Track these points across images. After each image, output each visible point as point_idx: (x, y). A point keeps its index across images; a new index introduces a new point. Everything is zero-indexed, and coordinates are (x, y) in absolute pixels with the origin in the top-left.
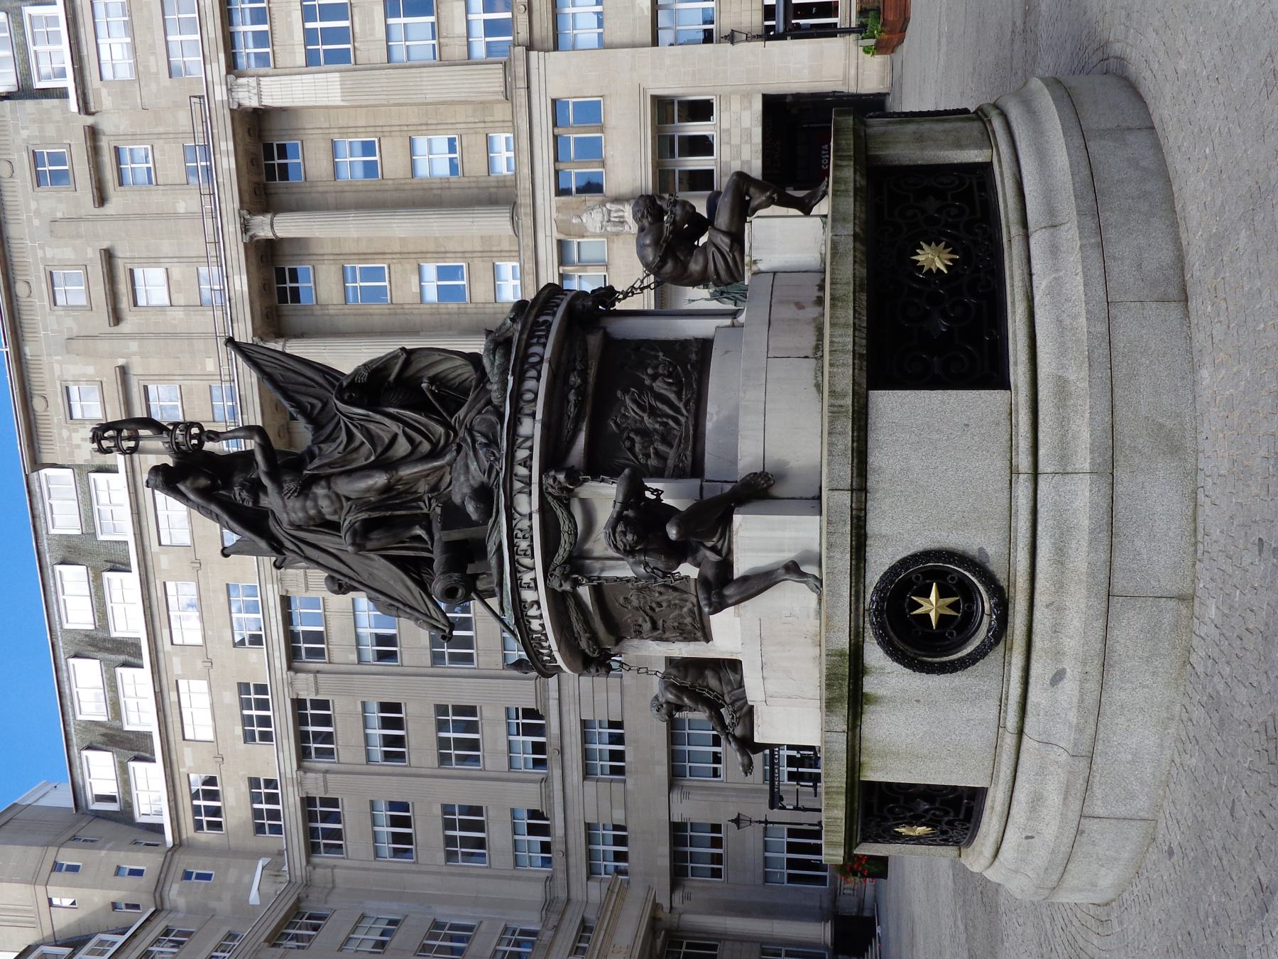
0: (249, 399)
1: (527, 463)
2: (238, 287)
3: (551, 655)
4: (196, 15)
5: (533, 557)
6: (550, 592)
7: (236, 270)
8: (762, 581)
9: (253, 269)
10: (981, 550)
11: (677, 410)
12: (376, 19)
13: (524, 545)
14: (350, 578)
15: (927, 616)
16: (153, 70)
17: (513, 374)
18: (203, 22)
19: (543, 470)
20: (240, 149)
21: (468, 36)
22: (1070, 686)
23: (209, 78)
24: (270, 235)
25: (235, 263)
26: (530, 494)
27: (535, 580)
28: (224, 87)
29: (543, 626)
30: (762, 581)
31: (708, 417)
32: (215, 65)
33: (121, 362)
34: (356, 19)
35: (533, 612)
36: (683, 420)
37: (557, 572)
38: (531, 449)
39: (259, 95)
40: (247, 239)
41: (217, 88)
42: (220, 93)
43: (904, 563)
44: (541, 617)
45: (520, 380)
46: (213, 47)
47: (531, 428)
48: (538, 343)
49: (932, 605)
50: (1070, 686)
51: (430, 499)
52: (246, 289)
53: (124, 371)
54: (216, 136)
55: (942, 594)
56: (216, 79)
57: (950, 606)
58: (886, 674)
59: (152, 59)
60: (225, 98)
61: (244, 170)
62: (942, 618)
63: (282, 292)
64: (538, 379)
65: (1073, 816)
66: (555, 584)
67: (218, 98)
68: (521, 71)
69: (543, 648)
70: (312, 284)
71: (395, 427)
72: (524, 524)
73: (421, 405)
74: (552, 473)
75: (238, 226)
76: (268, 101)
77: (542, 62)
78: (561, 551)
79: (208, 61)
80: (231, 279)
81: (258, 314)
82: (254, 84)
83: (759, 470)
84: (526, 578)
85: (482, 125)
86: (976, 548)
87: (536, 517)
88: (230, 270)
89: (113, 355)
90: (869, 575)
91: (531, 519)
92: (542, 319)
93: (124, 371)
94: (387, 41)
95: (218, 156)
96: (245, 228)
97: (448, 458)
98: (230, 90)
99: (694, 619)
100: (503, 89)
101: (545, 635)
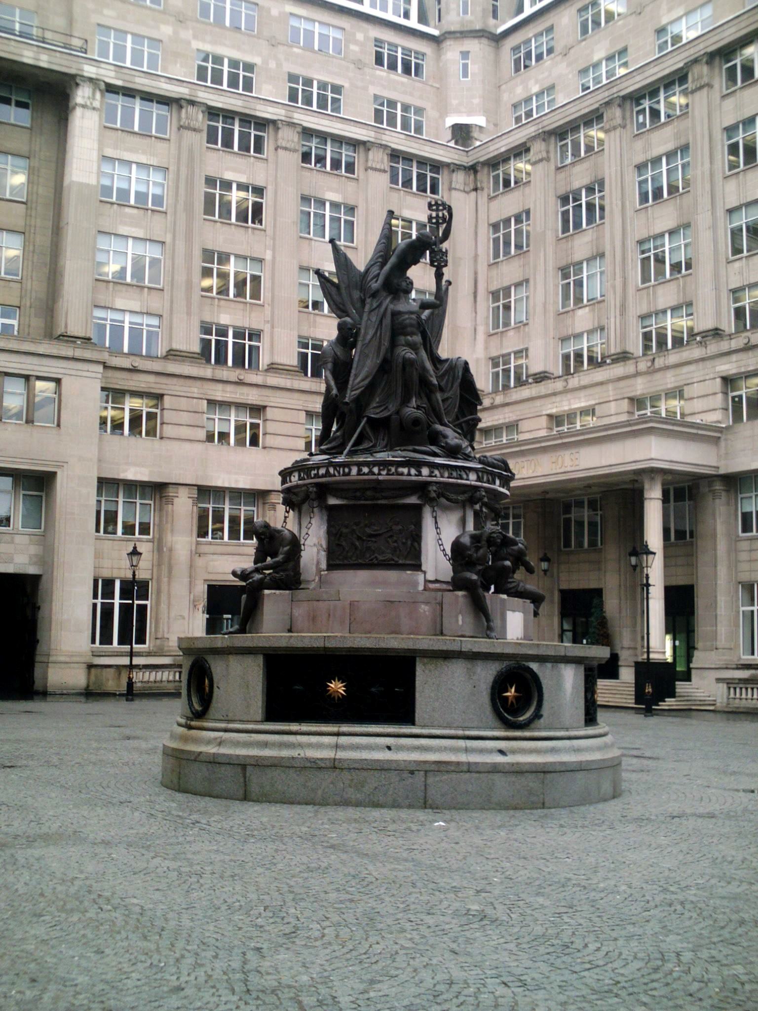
6: (430, 483)
12: (133, 229)
16: (106, 12)
19: (487, 490)
21: (111, 308)
22: (500, 759)
23: (103, 65)
27: (435, 476)
28: (93, 76)
32: (113, 74)
34: (135, 211)
35: (413, 471)
39: (84, 106)
42: (89, 70)
46: (127, 78)
49: (511, 693)
54: (53, 53)
56: (102, 72)
57: (512, 702)
58: (487, 673)
60: (86, 74)
65: (427, 767)
68: (87, 354)
69: (380, 470)
77: (94, 375)
79: (117, 69)
85: (28, 304)
94: (115, 234)
95: (35, 49)
98: (91, 80)
100: (69, 334)
101: (392, 474)
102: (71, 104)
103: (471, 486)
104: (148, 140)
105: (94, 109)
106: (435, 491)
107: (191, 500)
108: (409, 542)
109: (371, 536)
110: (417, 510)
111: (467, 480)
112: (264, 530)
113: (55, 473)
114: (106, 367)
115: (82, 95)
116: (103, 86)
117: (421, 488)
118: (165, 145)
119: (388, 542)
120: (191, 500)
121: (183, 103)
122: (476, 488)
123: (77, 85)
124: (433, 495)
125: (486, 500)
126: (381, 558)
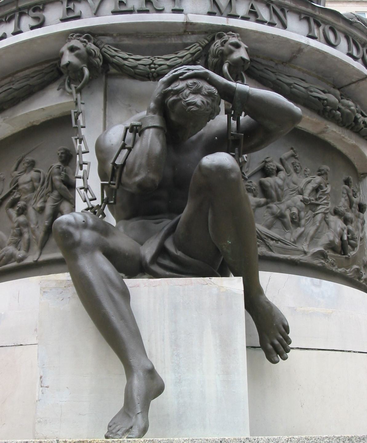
5: (115, 13)
26: (210, 13)
27: (78, 17)
30: (115, 333)
37: (91, 46)
38: (272, 24)
44: (17, 32)
83: (296, 337)
87: (179, 18)
91: (175, 11)
103: (189, 28)
119: (10, 217)
125: (242, 53)
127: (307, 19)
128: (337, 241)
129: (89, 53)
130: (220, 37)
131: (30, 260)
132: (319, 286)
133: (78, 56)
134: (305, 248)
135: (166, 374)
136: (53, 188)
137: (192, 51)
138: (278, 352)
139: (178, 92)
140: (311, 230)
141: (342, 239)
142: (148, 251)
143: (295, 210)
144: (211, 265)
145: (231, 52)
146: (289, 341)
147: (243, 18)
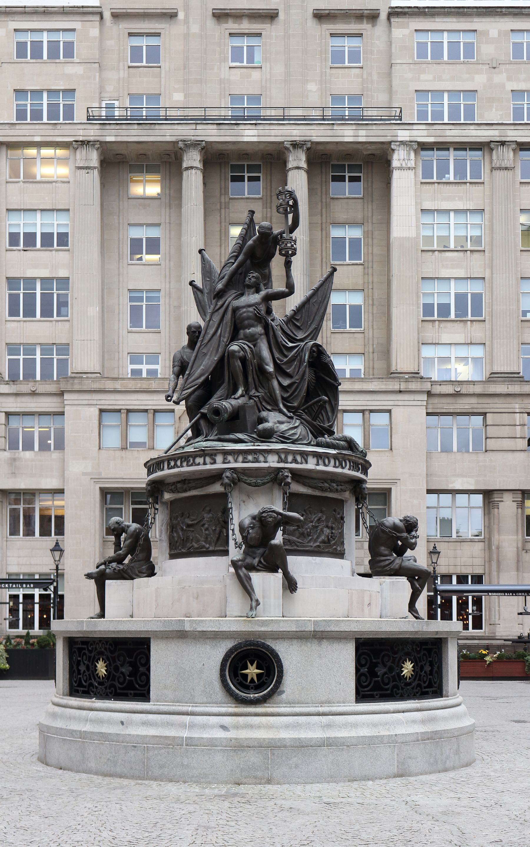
0: (151, 132)
1: (295, 461)
2: (247, 132)
3: (176, 466)
4: (462, 121)
5: (243, 462)
6: (224, 470)
7: (262, 133)
8: (247, 588)
9: (261, 147)
10: (283, 692)
11: (315, 541)
13: (250, 458)
14: (202, 341)
15: (247, 668)
17: (338, 453)
18: (458, 127)
19: (291, 470)
20: (359, 146)
23: (415, 127)
24: (290, 165)
25: (267, 132)
26: (278, 462)
27: (229, 462)
28: (408, 139)
29: (199, 464)
30: (247, 588)
31: (314, 558)
32: (425, 133)
33: (181, 15)
35: (208, 460)
36: (311, 544)
38: (302, 463)
39: (401, 168)
40: (287, 145)
41: (407, 133)
42: (403, 135)
43: (277, 656)
44: (205, 464)
45: (335, 457)
46: (438, 133)
47: (311, 465)
48: (350, 467)
49: (252, 671)
50: (221, 734)
51: (258, 396)
52: (246, 139)
53: (172, 16)
54: (370, 127)
55: (258, 675)
57: (252, 679)
59: (430, 77)
60: (400, 139)
61: (341, 148)
62: (246, 676)
63: (241, 168)
64: (335, 466)
66: (228, 474)
67: (400, 133)
70: (246, 196)
71: (296, 378)
72: (261, 458)
73: (309, 395)
74: (290, 475)
75: (297, 139)
76: (396, 175)
78: (245, 478)
80: (253, 127)
81: (224, 147)
82: (409, 165)
84: (230, 458)
86: (285, 689)
88: (261, 127)
89: (187, 8)
90: (270, 640)
91: (265, 462)
92: (360, 466)
93: (172, 16)
95: (354, 127)
96: (296, 145)
97: (285, 410)
99: (197, 548)
101: (192, 465)
102: (391, 169)
104: (463, 187)
105: (409, 168)
106: (227, 477)
107: (515, 504)
108: (218, 529)
109: (189, 526)
110: (223, 497)
111: (266, 462)
112: (117, 526)
113: (390, 489)
114: (429, 394)
115: (399, 158)
116: (415, 146)
117: (216, 476)
118: (480, 188)
119: (201, 530)
120: (515, 504)
121: (492, 145)
122: (279, 469)
123: (393, 150)
124: (226, 481)
126: (196, 546)
127: (317, 457)
128: (326, 539)
129: (233, 478)
130: (282, 472)
131: (211, 548)
132: (315, 560)
133: (229, 480)
134: (311, 544)
135: (261, 600)
136: (219, 523)
137: (271, 477)
138: (293, 590)
139: (265, 517)
140: (315, 536)
141: (328, 539)
142: (256, 561)
143: (309, 530)
144: (273, 569)
145: (285, 479)
146: (297, 587)
147: (291, 463)
